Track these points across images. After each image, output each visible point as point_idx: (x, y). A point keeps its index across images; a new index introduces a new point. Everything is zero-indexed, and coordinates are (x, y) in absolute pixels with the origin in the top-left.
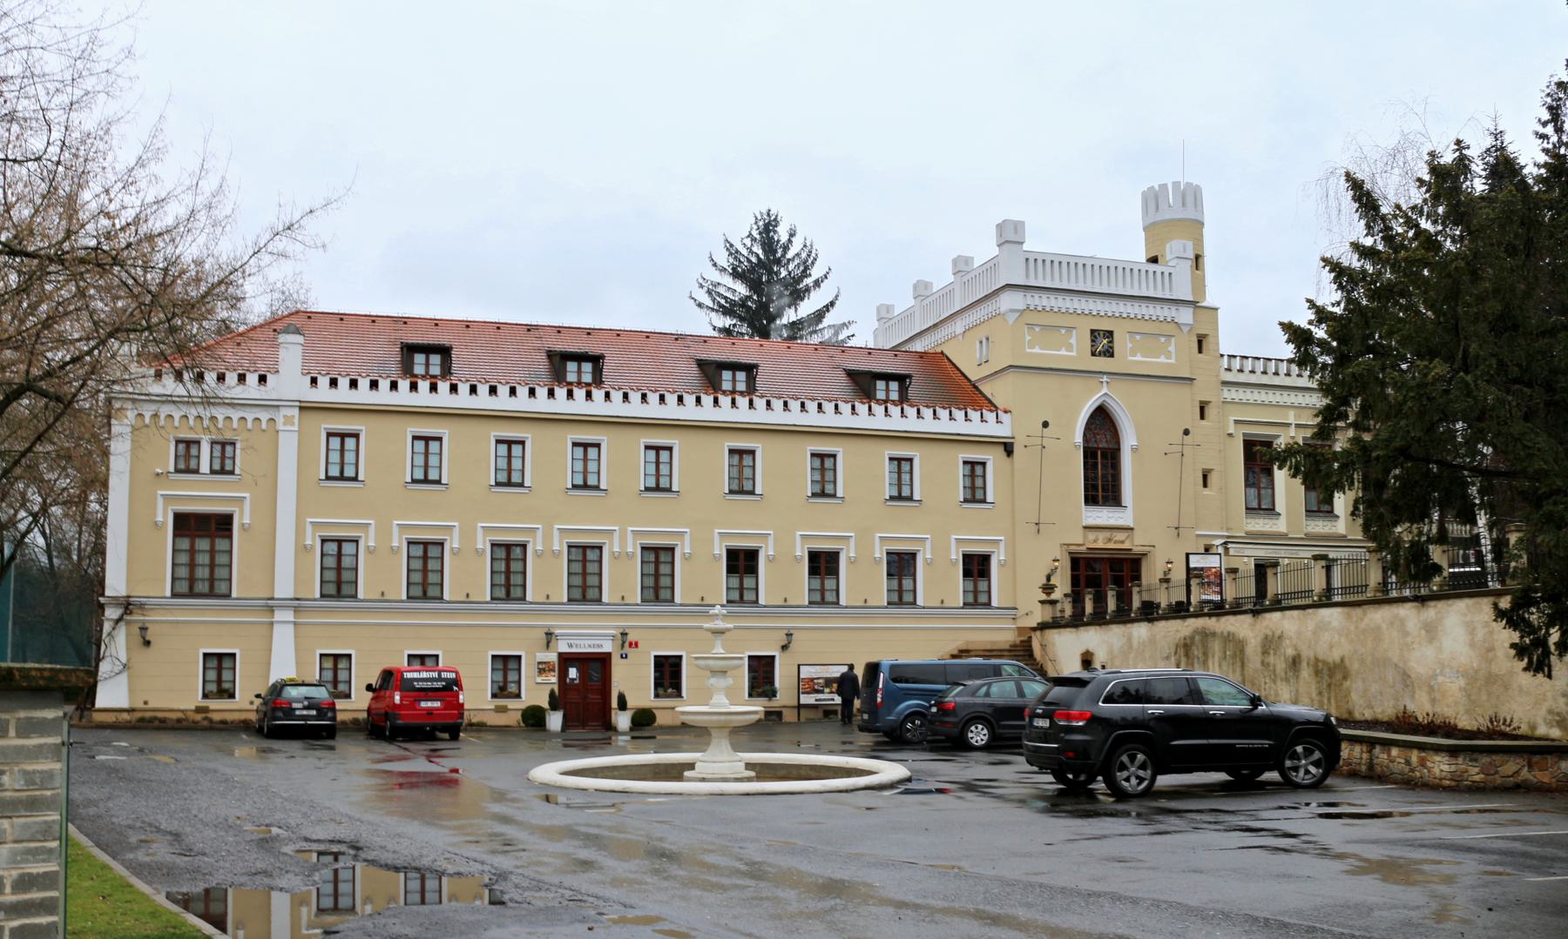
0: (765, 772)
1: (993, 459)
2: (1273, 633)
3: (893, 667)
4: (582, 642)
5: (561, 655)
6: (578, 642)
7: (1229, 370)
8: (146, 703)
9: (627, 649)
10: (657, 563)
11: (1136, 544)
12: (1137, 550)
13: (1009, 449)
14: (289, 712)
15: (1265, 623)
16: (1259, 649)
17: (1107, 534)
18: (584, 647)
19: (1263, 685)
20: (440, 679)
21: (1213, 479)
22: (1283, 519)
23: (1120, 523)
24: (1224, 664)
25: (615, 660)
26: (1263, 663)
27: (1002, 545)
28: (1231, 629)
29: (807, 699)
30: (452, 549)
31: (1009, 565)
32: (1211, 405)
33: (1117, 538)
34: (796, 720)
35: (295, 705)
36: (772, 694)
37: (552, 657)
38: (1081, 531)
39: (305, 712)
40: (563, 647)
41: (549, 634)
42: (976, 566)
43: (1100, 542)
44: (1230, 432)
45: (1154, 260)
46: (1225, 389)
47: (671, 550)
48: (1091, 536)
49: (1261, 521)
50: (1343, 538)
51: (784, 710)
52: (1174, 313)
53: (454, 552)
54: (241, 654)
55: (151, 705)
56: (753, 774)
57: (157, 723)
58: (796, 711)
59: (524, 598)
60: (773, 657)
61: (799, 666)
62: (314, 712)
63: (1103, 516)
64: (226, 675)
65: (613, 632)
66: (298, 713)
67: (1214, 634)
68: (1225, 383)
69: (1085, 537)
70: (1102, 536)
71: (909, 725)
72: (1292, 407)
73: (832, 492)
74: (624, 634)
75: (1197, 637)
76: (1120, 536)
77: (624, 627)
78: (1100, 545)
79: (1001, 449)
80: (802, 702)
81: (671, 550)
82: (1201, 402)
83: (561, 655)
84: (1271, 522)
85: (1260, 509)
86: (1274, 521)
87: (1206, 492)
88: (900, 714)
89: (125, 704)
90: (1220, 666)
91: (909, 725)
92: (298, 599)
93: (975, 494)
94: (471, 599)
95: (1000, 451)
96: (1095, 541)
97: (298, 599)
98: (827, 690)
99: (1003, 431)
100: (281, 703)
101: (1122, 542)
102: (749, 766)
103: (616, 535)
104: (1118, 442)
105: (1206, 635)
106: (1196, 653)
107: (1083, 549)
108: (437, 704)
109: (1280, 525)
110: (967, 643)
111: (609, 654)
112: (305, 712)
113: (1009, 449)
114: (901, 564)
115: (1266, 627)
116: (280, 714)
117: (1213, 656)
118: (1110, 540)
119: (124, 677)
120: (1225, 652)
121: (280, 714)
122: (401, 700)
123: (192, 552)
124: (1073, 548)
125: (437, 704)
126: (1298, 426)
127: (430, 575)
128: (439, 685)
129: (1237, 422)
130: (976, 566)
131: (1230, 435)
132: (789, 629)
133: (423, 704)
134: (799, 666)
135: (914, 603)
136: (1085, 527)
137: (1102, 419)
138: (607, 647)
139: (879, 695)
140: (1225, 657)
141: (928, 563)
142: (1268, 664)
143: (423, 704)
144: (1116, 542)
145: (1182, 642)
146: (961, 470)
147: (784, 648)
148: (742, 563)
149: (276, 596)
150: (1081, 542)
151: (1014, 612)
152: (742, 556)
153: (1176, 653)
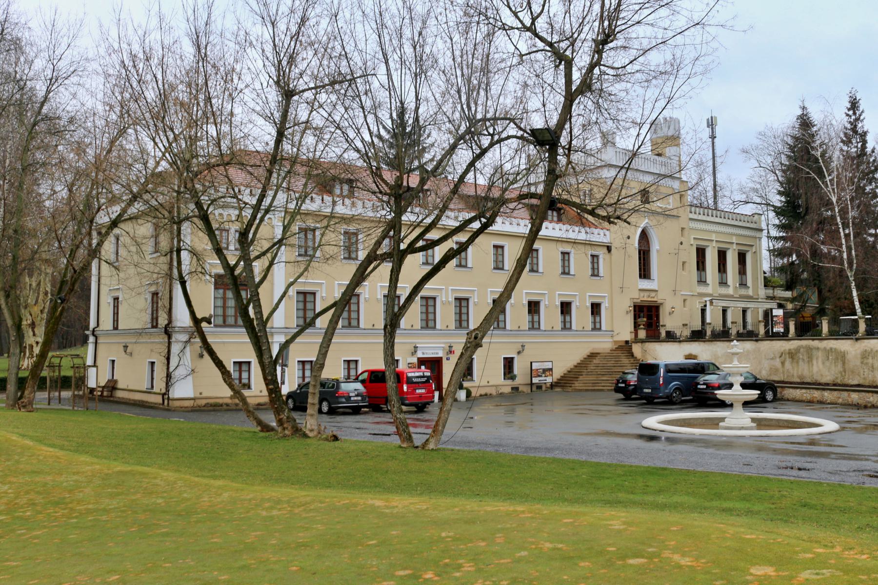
0: (761, 424)
1: (602, 253)
2: (872, 350)
3: (666, 365)
4: (429, 352)
5: (419, 359)
6: (429, 352)
7: (691, 212)
8: (201, 394)
9: (450, 356)
10: (305, 302)
11: (658, 298)
12: (660, 301)
13: (609, 249)
14: (348, 398)
15: (863, 345)
16: (859, 356)
18: (430, 354)
19: (862, 373)
20: (423, 377)
21: (687, 265)
22: (710, 286)
23: (652, 287)
24: (827, 364)
25: (444, 361)
26: (862, 363)
28: (834, 346)
29: (535, 380)
30: (365, 298)
31: (611, 308)
34: (529, 391)
35: (351, 394)
36: (513, 378)
37: (415, 360)
38: (637, 292)
39: (355, 398)
40: (420, 354)
41: (416, 347)
42: (596, 308)
45: (659, 155)
47: (467, 300)
48: (642, 294)
49: (702, 288)
50: (732, 296)
51: (520, 386)
52: (670, 183)
53: (475, 304)
54: (150, 358)
55: (204, 395)
56: (754, 425)
57: (225, 407)
58: (530, 386)
59: (435, 327)
60: (512, 358)
61: (531, 363)
62: (360, 398)
63: (645, 284)
64: (245, 375)
65: (443, 345)
66: (352, 399)
67: (818, 349)
68: (691, 219)
69: (639, 295)
70: (646, 294)
71: (674, 395)
72: (714, 232)
73: (501, 266)
74: (450, 347)
75: (802, 350)
76: (653, 294)
77: (450, 343)
78: (645, 299)
79: (606, 248)
80: (533, 382)
81: (467, 300)
83: (419, 359)
84: (705, 288)
87: (684, 273)
88: (671, 389)
89: (192, 395)
90: (823, 363)
91: (674, 395)
92: (287, 328)
93: (595, 273)
94: (375, 327)
95: (605, 250)
97: (287, 328)
98: (543, 375)
99: (606, 240)
100: (343, 393)
101: (654, 297)
102: (753, 420)
103: (444, 292)
104: (649, 247)
105: (809, 350)
106: (801, 357)
107: (639, 301)
108: (423, 391)
109: (730, 291)
110: (593, 349)
111: (441, 358)
112: (355, 398)
113: (609, 249)
114: (566, 307)
115: (866, 346)
116: (344, 400)
117: (817, 359)
118: (649, 296)
119: (190, 378)
120: (828, 357)
121: (344, 400)
122: (407, 389)
123: (224, 299)
124: (635, 301)
125: (423, 391)
126: (717, 241)
127: (352, 313)
128: (424, 380)
129: (694, 238)
130: (596, 308)
131: (692, 245)
132: (523, 342)
133: (418, 391)
134: (531, 363)
135: (570, 328)
137: (644, 236)
138: (440, 354)
139: (661, 379)
140: (828, 359)
141: (577, 307)
142: (867, 364)
143: (418, 391)
145: (787, 351)
146: (560, 256)
147: (519, 353)
148: (533, 308)
149: (275, 326)
151: (612, 333)
152: (645, 310)
153: (780, 357)
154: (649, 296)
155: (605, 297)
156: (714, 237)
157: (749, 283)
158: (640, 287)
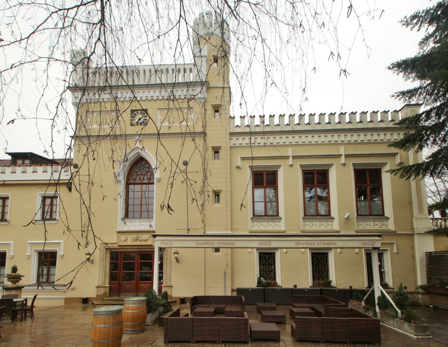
17: (135, 236)
22: (283, 221)
27: (62, 246)
32: (222, 149)
33: (140, 239)
43: (130, 241)
44: (239, 165)
46: (234, 138)
48: (123, 237)
68: (232, 134)
72: (291, 145)
78: (129, 243)
82: (214, 148)
85: (266, 215)
86: (277, 223)
87: (217, 205)
96: (125, 241)
101: (146, 241)
107: (116, 246)
118: (136, 240)
126: (294, 157)
129: (243, 159)
131: (238, 167)
136: (118, 232)
144: (140, 241)
150: (116, 242)
154: (136, 240)
155: (59, 243)
156: (290, 152)
157: (389, 211)
158: (126, 228)
